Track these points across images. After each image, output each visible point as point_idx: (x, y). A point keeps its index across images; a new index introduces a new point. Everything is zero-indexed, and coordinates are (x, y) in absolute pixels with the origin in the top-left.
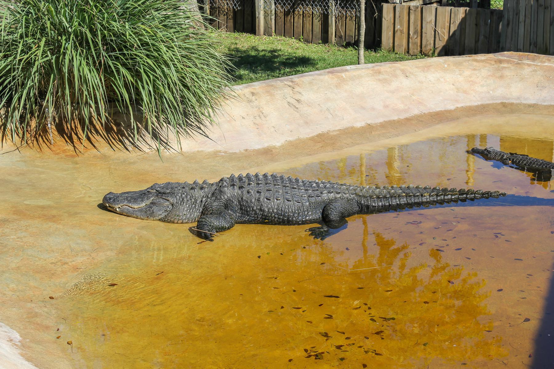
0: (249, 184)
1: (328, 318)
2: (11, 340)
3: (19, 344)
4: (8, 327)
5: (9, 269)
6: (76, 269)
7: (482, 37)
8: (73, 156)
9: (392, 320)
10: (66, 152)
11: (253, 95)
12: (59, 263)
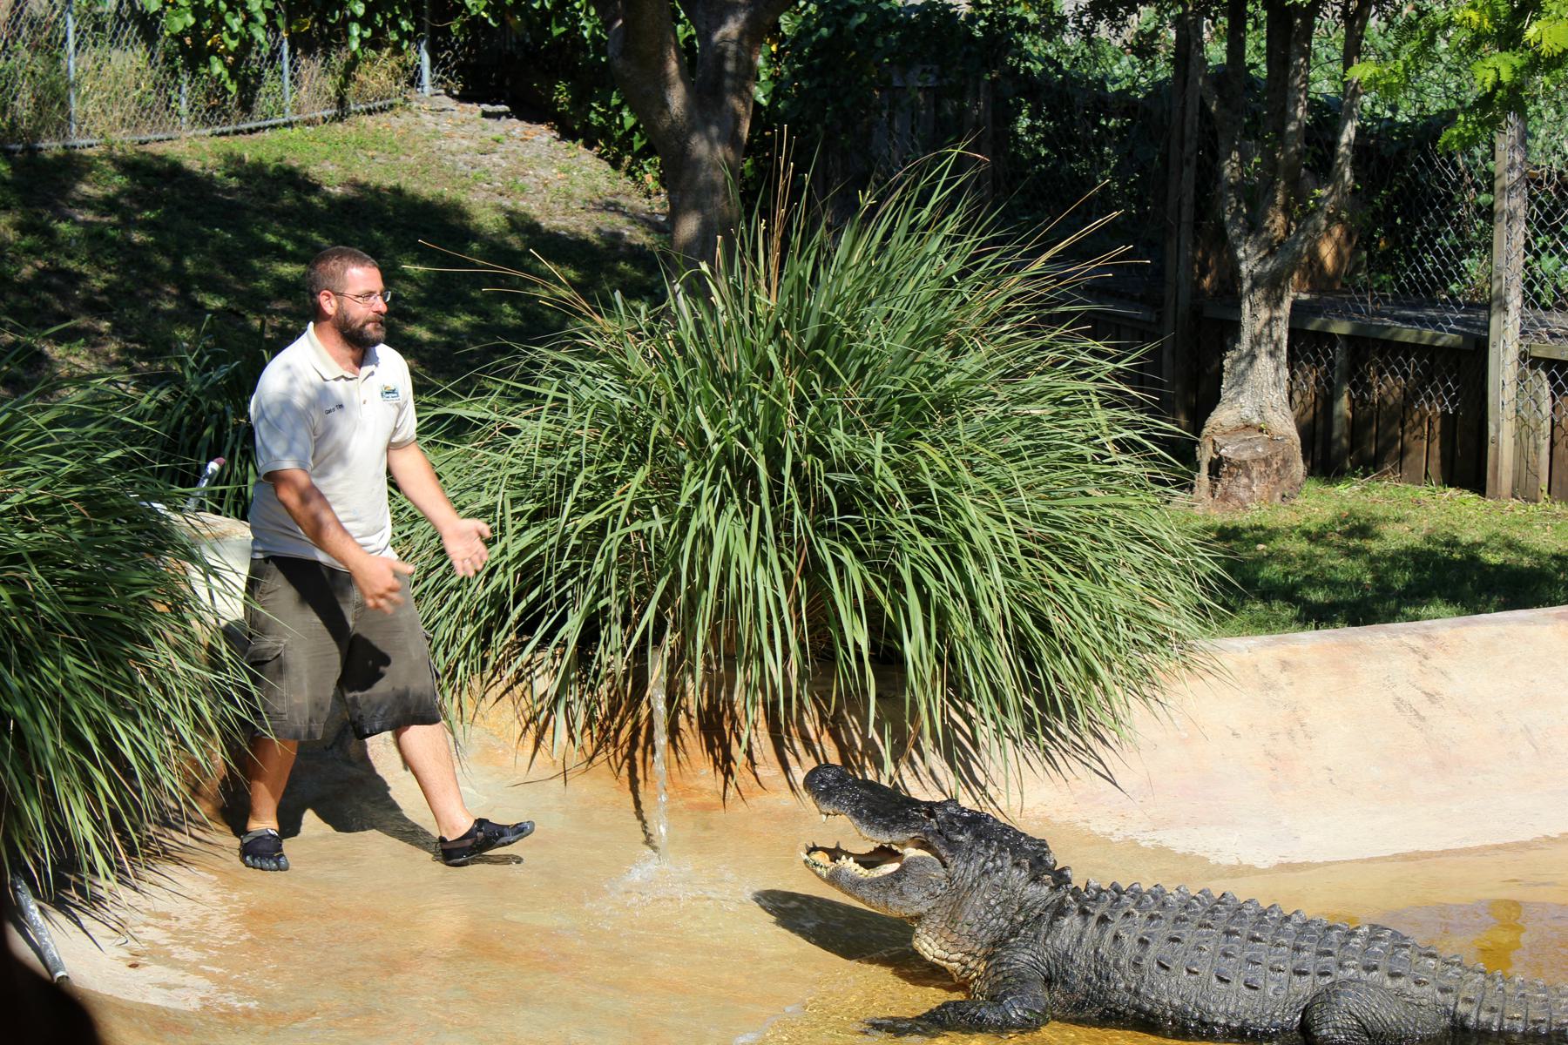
8: (706, 807)
10: (691, 795)
11: (1284, 669)
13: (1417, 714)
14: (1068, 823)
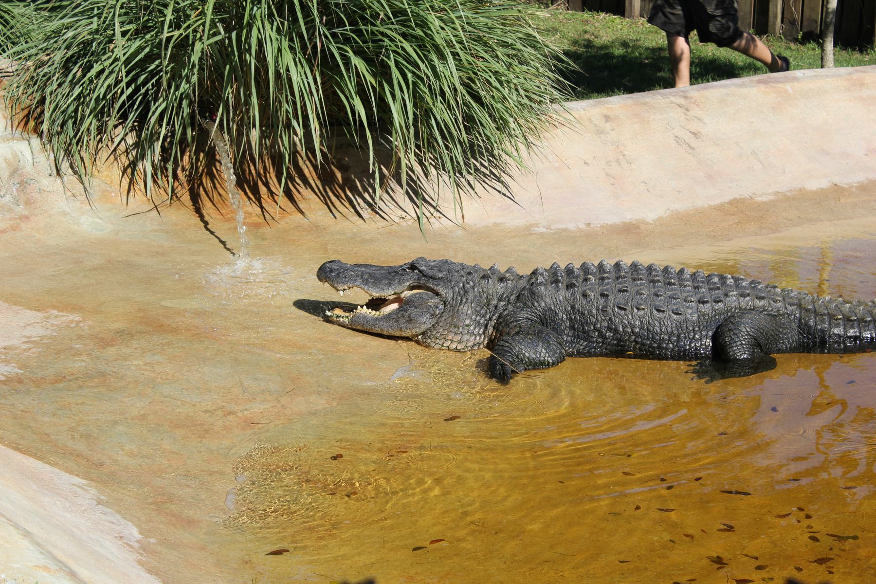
0: (586, 280)
1: (728, 530)
2: (122, 538)
3: (137, 545)
4: (118, 516)
5: (127, 419)
6: (250, 423)
8: (257, 226)
9: (851, 540)
11: (607, 121)
12: (220, 413)
13: (689, 146)
14: (496, 224)
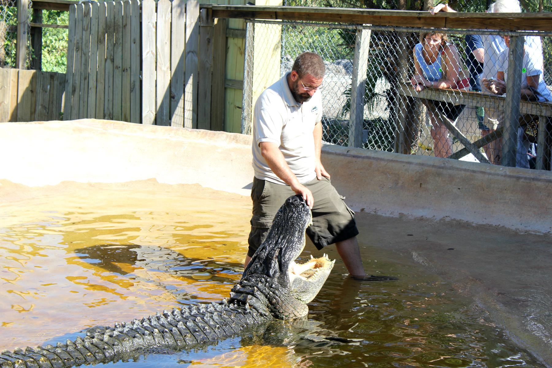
7: (40, 107)
